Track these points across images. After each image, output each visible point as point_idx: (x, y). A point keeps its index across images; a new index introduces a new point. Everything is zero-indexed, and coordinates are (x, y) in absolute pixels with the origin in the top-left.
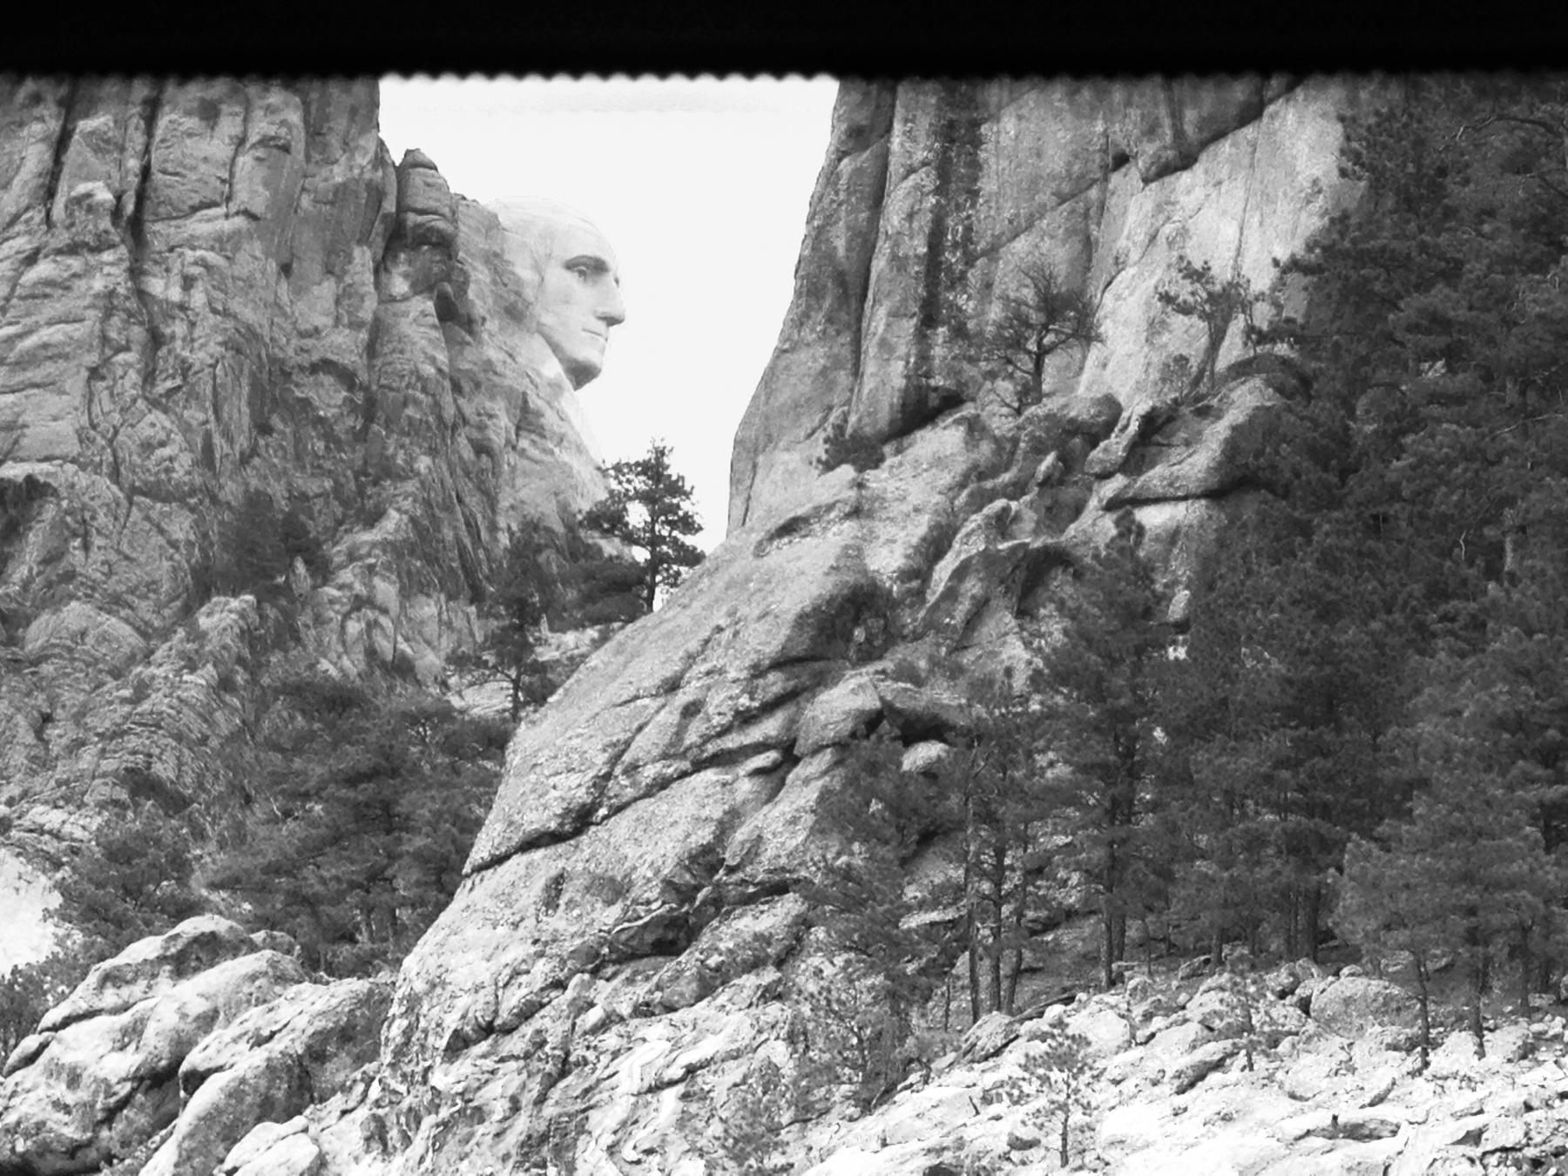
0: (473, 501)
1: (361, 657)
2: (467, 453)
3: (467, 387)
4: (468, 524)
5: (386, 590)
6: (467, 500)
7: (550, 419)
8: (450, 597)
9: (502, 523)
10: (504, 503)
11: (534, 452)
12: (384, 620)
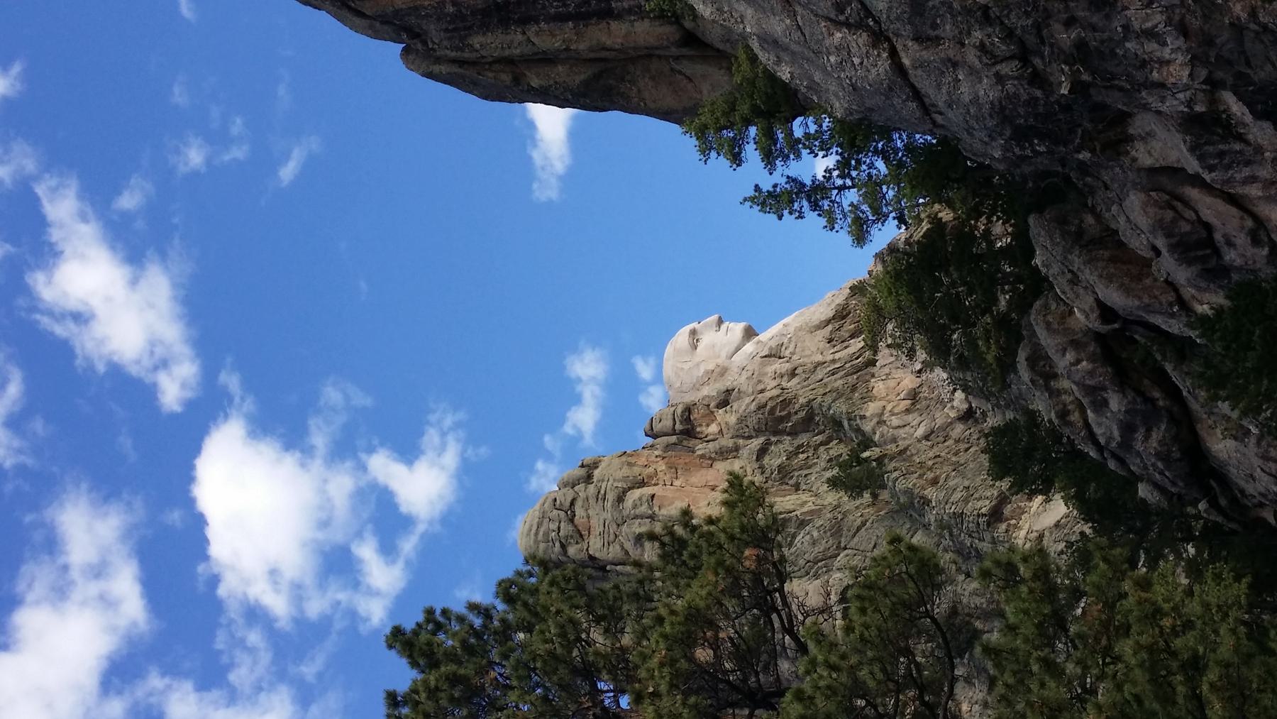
0: (820, 374)
2: (795, 380)
3: (760, 387)
5: (872, 408)
7: (773, 344)
8: (873, 376)
9: (831, 357)
10: (819, 358)
11: (791, 349)
12: (889, 408)
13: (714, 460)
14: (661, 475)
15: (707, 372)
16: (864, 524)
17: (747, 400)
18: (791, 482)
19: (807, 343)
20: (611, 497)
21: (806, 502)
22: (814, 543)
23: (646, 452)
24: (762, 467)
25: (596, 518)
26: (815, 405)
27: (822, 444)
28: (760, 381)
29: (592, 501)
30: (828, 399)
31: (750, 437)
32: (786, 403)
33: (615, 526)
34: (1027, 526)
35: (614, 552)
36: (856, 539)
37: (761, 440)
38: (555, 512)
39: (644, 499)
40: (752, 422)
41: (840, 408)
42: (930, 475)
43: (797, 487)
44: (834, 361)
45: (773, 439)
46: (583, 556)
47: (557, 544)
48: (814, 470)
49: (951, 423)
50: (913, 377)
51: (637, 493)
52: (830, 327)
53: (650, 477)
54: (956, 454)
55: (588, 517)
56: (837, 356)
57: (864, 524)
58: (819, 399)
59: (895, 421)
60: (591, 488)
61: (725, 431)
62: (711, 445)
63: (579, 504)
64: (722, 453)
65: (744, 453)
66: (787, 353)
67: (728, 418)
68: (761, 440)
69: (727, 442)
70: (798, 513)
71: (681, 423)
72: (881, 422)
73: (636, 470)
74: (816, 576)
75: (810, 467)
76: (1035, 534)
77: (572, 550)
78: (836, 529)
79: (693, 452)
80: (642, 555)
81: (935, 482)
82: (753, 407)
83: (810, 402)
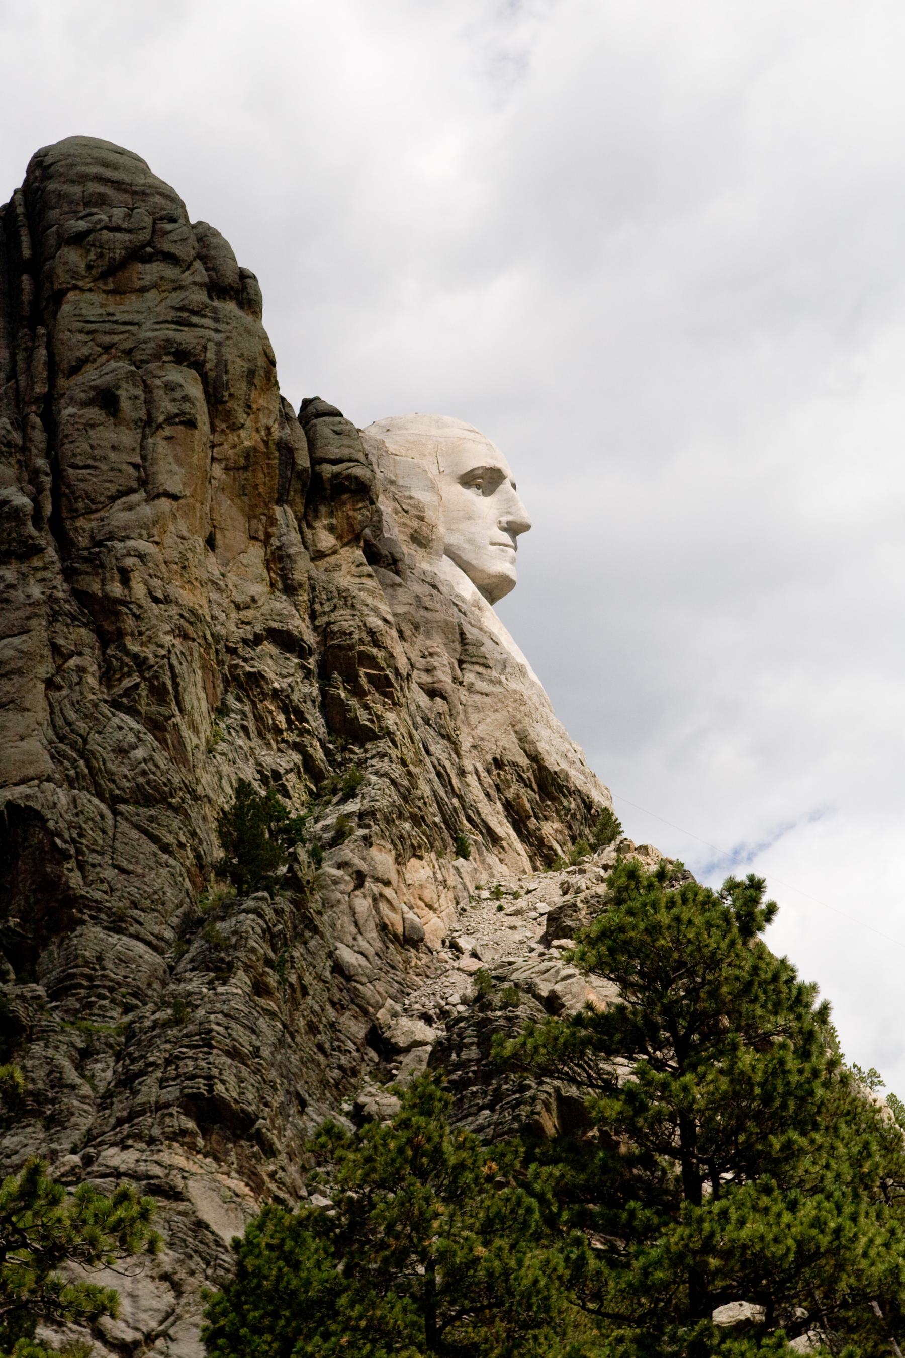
0: (439, 748)
1: (374, 934)
2: (423, 699)
3: (407, 630)
4: (439, 774)
5: (382, 858)
6: (432, 749)
7: (488, 648)
8: (440, 855)
9: (468, 766)
10: (466, 743)
12: (388, 892)
13: (266, 542)
14: (232, 438)
15: (419, 507)
16: (166, 848)
17: (384, 608)
18: (231, 700)
19: (492, 717)
20: (186, 337)
21: (196, 731)
22: (122, 751)
23: (276, 406)
24: (258, 640)
25: (146, 313)
26: (383, 745)
27: (308, 760)
28: (417, 627)
29: (176, 298)
30: (397, 771)
31: (313, 616)
32: (382, 685)
33: (128, 345)
34: (194, 1169)
35: (74, 343)
36: (135, 834)
37: (310, 638)
38: (148, 220)
39: (186, 407)
40: (344, 620)
41: (378, 792)
42: (272, 979)
43: (222, 711)
44: (462, 773)
45: (312, 663)
46: (62, 278)
47: (82, 225)
48: (256, 742)
49: (365, 1013)
50: (443, 934)
51: (195, 391)
52: (524, 761)
53: (228, 416)
54: (312, 1029)
55: (143, 290)
56: (472, 779)
57: (166, 848)
58: (394, 753)
59: (363, 904)
60: (199, 297)
61: (323, 564)
62: (295, 537)
63: (170, 272)
64: (280, 559)
65: (282, 604)
66: (469, 677)
67: (348, 569)
68: (310, 638)
69: (303, 568)
70: (178, 719)
71: (336, 476)
72: (360, 878)
73: (240, 388)
74: (57, 757)
75: (261, 735)
76: (179, 1183)
77: (73, 256)
78: (152, 795)
79: (280, 502)
80: (72, 401)
81: (260, 989)
82: (374, 621)
83: (389, 734)
